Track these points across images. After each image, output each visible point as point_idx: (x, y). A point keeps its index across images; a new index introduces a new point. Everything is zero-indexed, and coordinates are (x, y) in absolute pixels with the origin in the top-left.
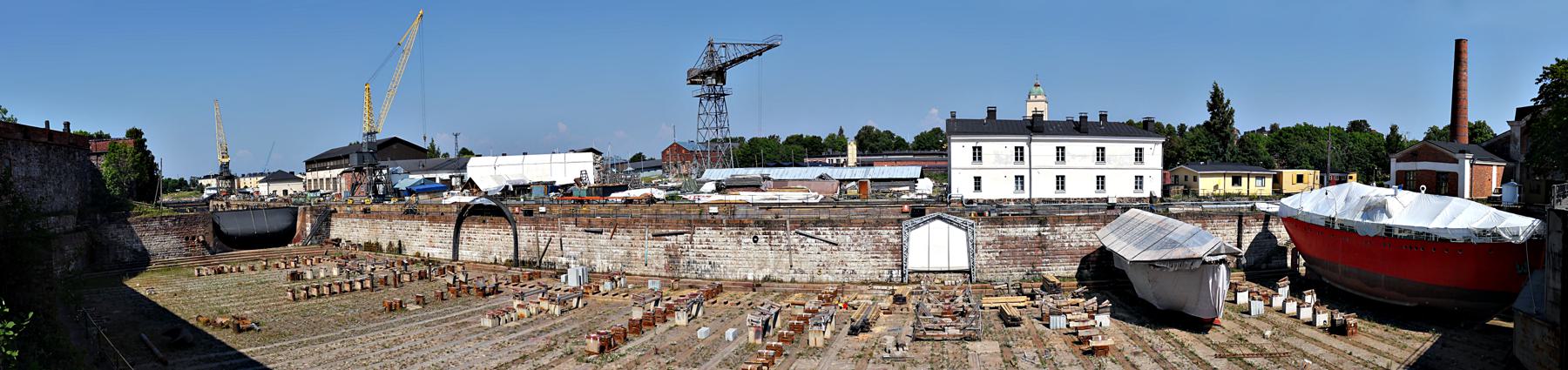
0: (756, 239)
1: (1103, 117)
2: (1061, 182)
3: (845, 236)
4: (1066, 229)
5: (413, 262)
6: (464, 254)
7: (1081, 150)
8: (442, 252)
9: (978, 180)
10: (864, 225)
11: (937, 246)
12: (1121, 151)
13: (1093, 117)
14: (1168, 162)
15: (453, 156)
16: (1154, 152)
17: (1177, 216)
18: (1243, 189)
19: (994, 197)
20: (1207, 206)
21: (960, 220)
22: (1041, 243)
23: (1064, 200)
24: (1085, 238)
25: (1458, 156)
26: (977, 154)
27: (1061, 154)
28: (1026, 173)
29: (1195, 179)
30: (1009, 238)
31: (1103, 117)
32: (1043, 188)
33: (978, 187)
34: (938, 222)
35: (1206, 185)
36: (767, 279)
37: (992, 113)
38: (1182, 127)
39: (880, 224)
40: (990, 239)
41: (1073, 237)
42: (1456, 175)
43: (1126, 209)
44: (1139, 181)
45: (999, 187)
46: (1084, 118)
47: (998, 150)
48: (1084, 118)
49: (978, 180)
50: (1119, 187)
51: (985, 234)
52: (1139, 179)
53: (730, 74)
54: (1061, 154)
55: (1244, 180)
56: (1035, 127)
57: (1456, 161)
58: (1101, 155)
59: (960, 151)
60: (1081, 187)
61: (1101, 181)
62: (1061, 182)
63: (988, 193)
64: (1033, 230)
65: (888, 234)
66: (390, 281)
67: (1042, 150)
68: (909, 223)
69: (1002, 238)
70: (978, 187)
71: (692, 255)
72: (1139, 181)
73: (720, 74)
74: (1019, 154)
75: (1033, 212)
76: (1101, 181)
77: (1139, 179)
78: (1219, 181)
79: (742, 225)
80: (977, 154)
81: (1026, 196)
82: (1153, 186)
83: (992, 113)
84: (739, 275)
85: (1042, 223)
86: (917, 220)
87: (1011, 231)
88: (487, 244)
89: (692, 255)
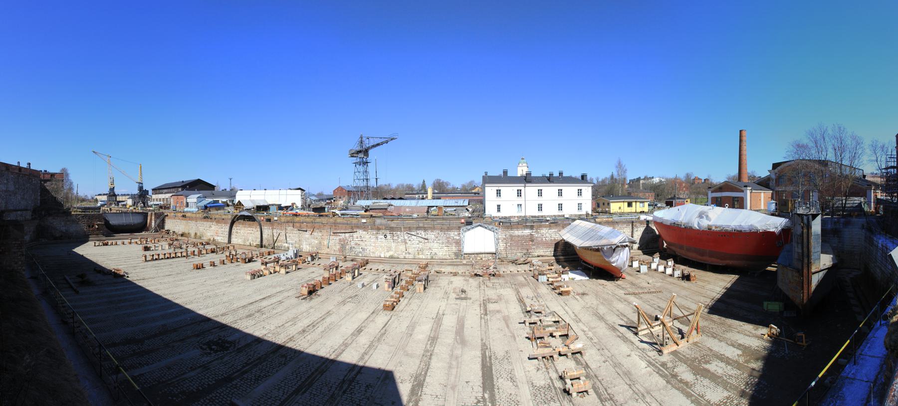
0: (385, 236)
1: (561, 174)
2: (540, 207)
3: (431, 235)
4: (544, 231)
5: (208, 244)
6: (234, 240)
7: (550, 190)
8: (222, 239)
9: (499, 206)
10: (441, 229)
11: (479, 240)
12: (570, 190)
13: (556, 174)
14: (595, 195)
15: (228, 190)
16: (587, 191)
17: (600, 223)
18: (633, 209)
19: (507, 215)
20: (615, 218)
21: (490, 227)
22: (532, 239)
24: (553, 235)
25: (744, 189)
26: (499, 193)
27: (540, 193)
28: (523, 203)
29: (608, 204)
31: (561, 174)
33: (499, 210)
34: (480, 228)
35: (615, 207)
36: (391, 257)
37: (505, 172)
38: (597, 179)
39: (449, 229)
43: (574, 220)
45: (510, 210)
46: (551, 175)
47: (509, 191)
48: (551, 175)
49: (499, 206)
50: (570, 210)
51: (502, 234)
52: (580, 205)
53: (371, 152)
54: (540, 193)
55: (634, 204)
56: (527, 179)
57: (742, 191)
58: (560, 193)
59: (490, 191)
60: (550, 210)
61: (560, 207)
62: (540, 207)
64: (527, 232)
65: (453, 234)
66: (196, 253)
67: (531, 190)
68: (464, 228)
69: (511, 236)
70: (499, 210)
71: (353, 244)
73: (366, 152)
74: (519, 193)
75: (525, 222)
76: (560, 207)
77: (580, 205)
78: (621, 204)
79: (379, 229)
80: (499, 193)
81: (523, 215)
82: (588, 208)
83: (505, 172)
84: (377, 254)
85: (532, 227)
86: (469, 227)
88: (246, 235)
89: (353, 244)
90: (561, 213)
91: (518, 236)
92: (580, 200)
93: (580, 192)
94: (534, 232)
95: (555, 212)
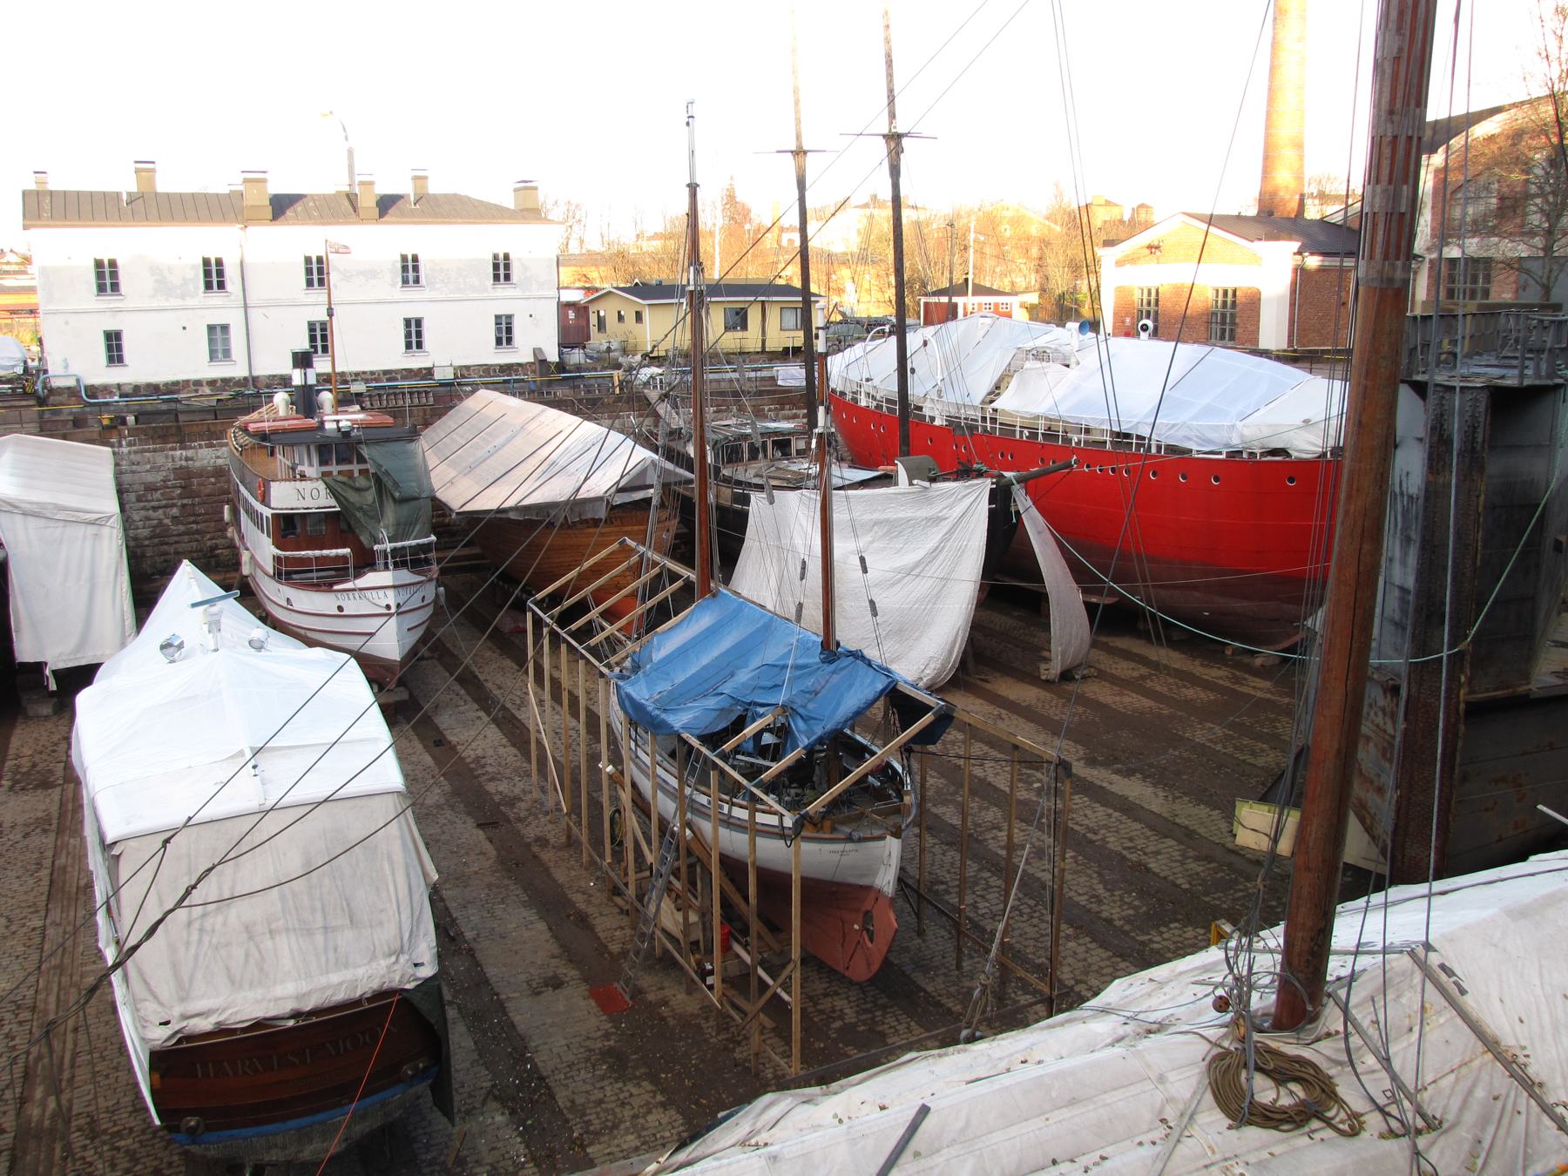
9: (113, 340)
30: (201, 473)
40: (156, 478)
44: (505, 332)
49: (113, 340)
61: (414, 333)
63: (141, 368)
72: (505, 332)
76: (414, 333)
81: (236, 369)
90: (416, 362)
92: (504, 300)
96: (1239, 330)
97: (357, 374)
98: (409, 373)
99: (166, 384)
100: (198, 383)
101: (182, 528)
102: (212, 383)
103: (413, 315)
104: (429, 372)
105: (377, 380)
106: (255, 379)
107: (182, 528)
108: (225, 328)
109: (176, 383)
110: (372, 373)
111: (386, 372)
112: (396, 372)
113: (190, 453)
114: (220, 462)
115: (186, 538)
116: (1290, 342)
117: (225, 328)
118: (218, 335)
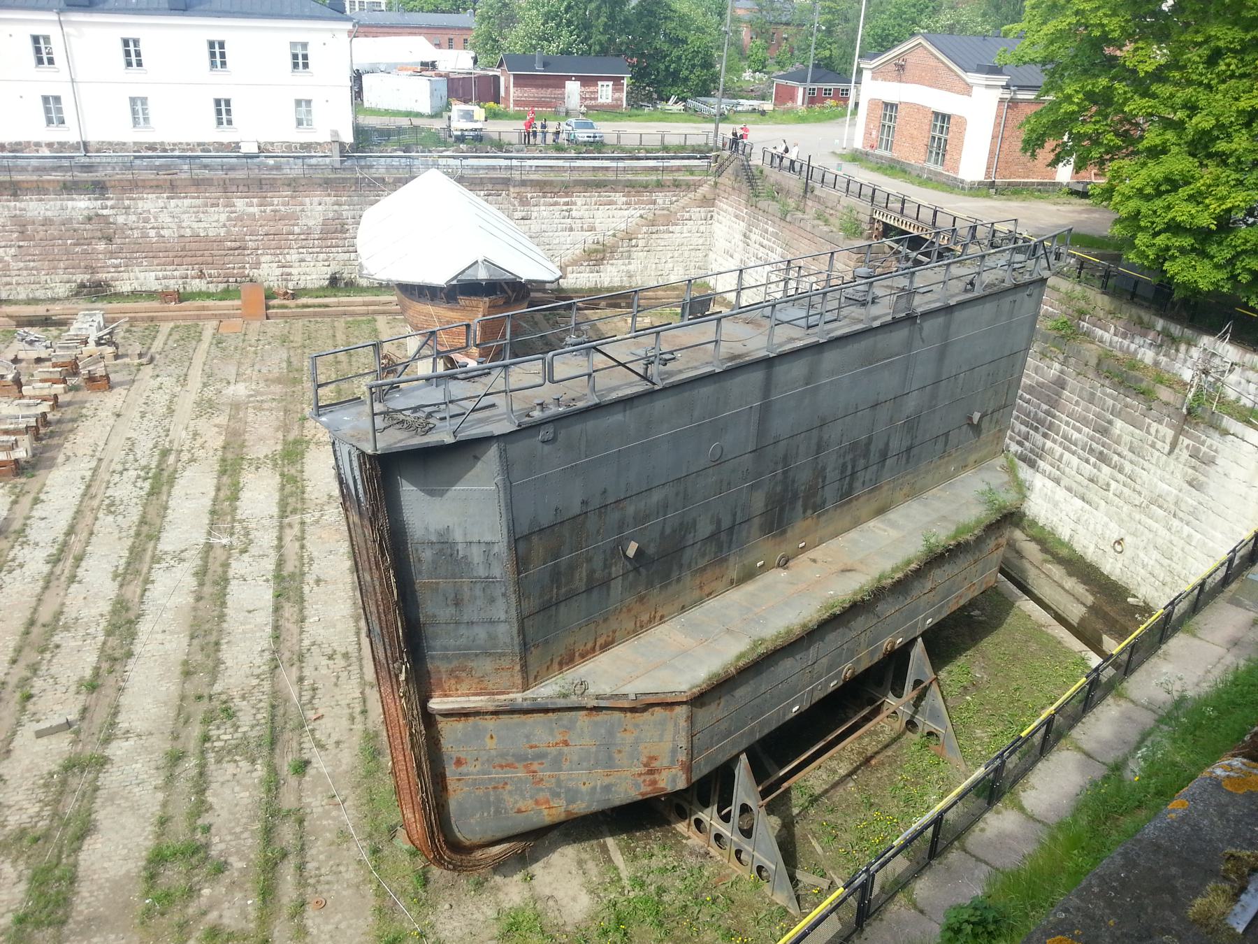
4: (150, 203)
23: (152, 147)
24: (188, 220)
25: (972, 78)
32: (101, 121)
41: (165, 218)
42: (962, 122)
57: (967, 89)
60: (182, 122)
61: (223, 108)
64: (82, 205)
76: (223, 108)
81: (69, 134)
85: (99, 188)
87: (34, 207)
91: (47, 222)
92: (302, 84)
93: (300, 61)
94: (106, 207)
95: (199, 128)
96: (947, 157)
97: (174, 144)
98: (221, 146)
99: (10, 144)
100: (38, 144)
101: (22, 265)
102: (50, 145)
103: (222, 95)
104: (237, 146)
105: (192, 150)
106: (85, 144)
107: (22, 265)
108: (57, 99)
109: (19, 144)
110: (188, 144)
111: (199, 144)
112: (209, 144)
113: (23, 205)
114: (49, 214)
115: (25, 273)
116: (988, 174)
117: (57, 99)
118: (52, 105)
